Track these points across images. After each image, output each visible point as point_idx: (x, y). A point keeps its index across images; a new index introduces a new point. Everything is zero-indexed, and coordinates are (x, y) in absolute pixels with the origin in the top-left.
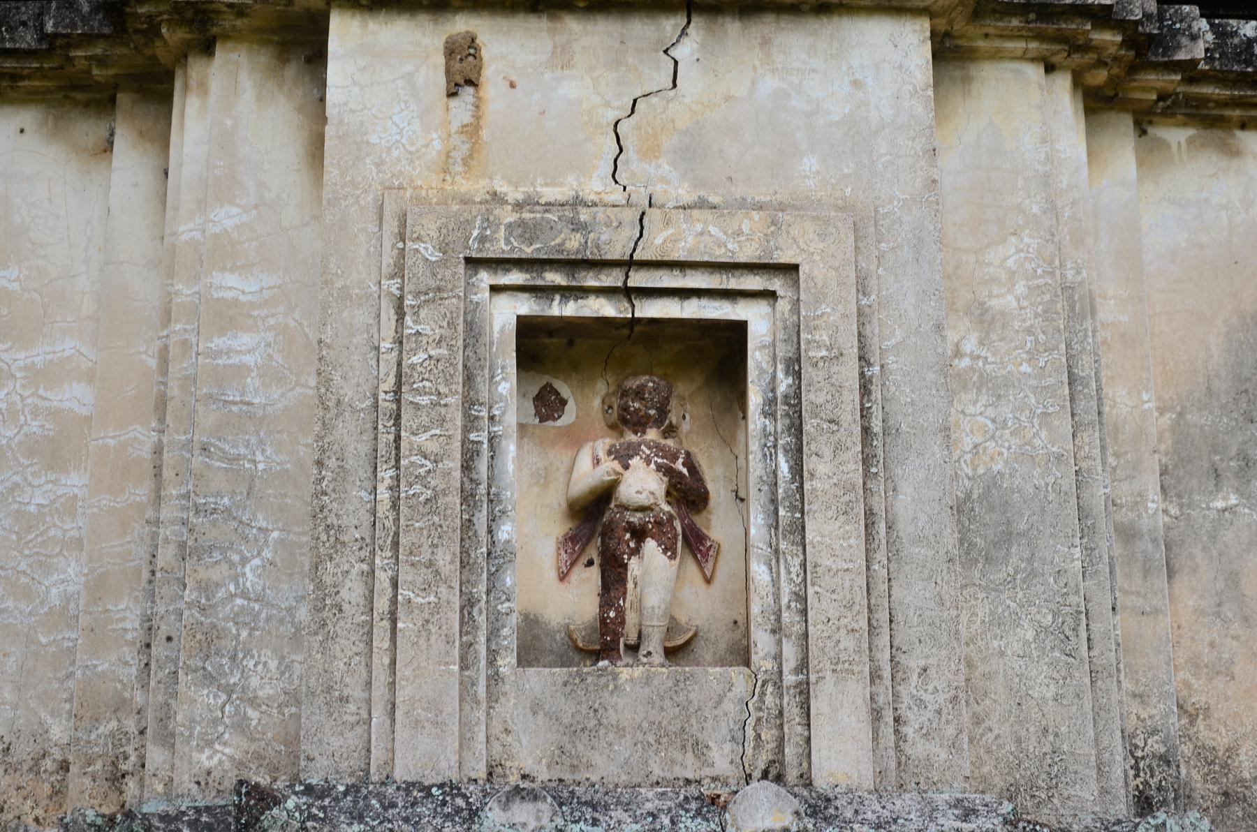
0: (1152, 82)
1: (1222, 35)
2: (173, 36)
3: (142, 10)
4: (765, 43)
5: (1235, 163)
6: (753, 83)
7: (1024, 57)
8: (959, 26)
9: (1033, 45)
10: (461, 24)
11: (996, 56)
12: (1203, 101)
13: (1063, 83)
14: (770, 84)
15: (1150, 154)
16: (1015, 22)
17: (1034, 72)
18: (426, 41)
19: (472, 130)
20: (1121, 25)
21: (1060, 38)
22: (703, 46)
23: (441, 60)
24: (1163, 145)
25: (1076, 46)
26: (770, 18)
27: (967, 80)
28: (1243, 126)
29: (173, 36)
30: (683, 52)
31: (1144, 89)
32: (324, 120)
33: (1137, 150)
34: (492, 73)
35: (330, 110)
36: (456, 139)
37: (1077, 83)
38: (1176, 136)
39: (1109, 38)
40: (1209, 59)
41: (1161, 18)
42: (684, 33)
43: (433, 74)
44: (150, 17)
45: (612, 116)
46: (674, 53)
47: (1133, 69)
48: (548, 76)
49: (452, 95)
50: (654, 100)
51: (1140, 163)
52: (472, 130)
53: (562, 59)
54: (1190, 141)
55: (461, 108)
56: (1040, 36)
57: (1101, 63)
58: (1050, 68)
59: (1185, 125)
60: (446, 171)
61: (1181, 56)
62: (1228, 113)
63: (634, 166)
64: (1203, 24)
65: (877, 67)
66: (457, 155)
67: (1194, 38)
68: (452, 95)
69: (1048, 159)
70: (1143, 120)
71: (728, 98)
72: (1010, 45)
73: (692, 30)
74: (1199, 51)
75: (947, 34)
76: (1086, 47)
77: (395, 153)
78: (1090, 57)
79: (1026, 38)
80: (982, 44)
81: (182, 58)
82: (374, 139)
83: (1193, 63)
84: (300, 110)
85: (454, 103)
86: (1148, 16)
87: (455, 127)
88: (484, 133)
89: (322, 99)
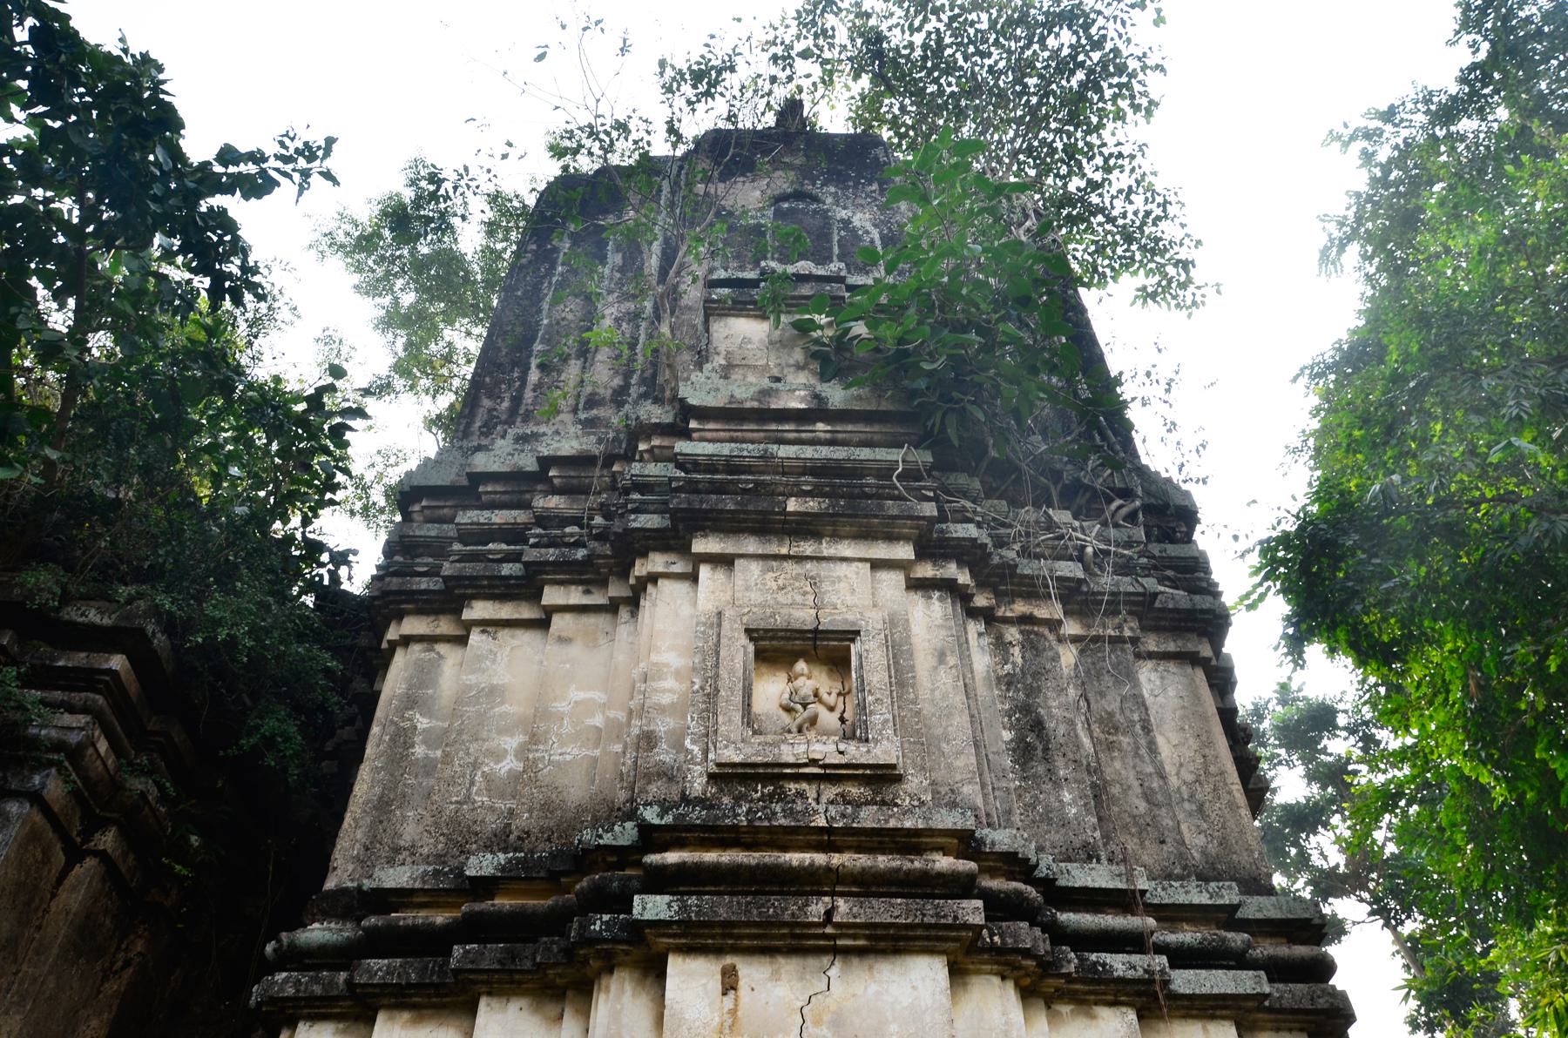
0: (1051, 984)
1: (1082, 960)
2: (594, 964)
3: (581, 952)
4: (871, 968)
5: (1094, 1022)
6: (866, 988)
7: (991, 973)
8: (960, 958)
9: (995, 967)
10: (729, 960)
11: (978, 972)
12: (1076, 992)
13: (1010, 985)
14: (873, 988)
15: (1054, 1018)
16: (986, 956)
17: (996, 980)
18: (713, 968)
19: (733, 1012)
20: (1035, 957)
21: (1007, 964)
22: (841, 970)
23: (719, 977)
24: (1059, 1013)
25: (1015, 967)
26: (872, 956)
27: (965, 984)
28: (1096, 1004)
29: (594, 964)
30: (833, 972)
31: (1049, 987)
32: (664, 1007)
33: (1047, 1016)
34: (743, 984)
35: (667, 1002)
36: (726, 1017)
37: (1017, 985)
38: (1065, 1009)
39: (1030, 963)
40: (1077, 972)
41: (1053, 952)
42: (832, 964)
43: (716, 984)
44: (585, 955)
45: (799, 1004)
46: (828, 973)
47: (1042, 977)
48: (769, 985)
49: (724, 994)
50: (819, 996)
51: (1049, 1023)
52: (733, 1012)
53: (776, 977)
54: (1072, 1011)
55: (728, 1001)
56: (997, 963)
57: (1027, 975)
58: (1003, 978)
59: (1068, 1003)
60: (721, 1033)
61: (1064, 971)
62: (1087, 997)
63: (810, 1030)
64: (1072, 955)
65: (923, 979)
66: (726, 1025)
67: (1069, 962)
68: (724, 994)
69: (1006, 1023)
70: (1049, 1002)
71: (854, 995)
72: (984, 967)
73: (836, 962)
74: (1072, 968)
75: (955, 962)
76: (1020, 968)
77: (697, 1024)
78: (1022, 972)
79: (992, 964)
80: (971, 967)
81: (598, 975)
82: (687, 1017)
83: (1070, 974)
84: (652, 1000)
85: (725, 998)
86: (1046, 952)
87: (726, 1010)
88: (739, 1013)
89: (663, 995)
